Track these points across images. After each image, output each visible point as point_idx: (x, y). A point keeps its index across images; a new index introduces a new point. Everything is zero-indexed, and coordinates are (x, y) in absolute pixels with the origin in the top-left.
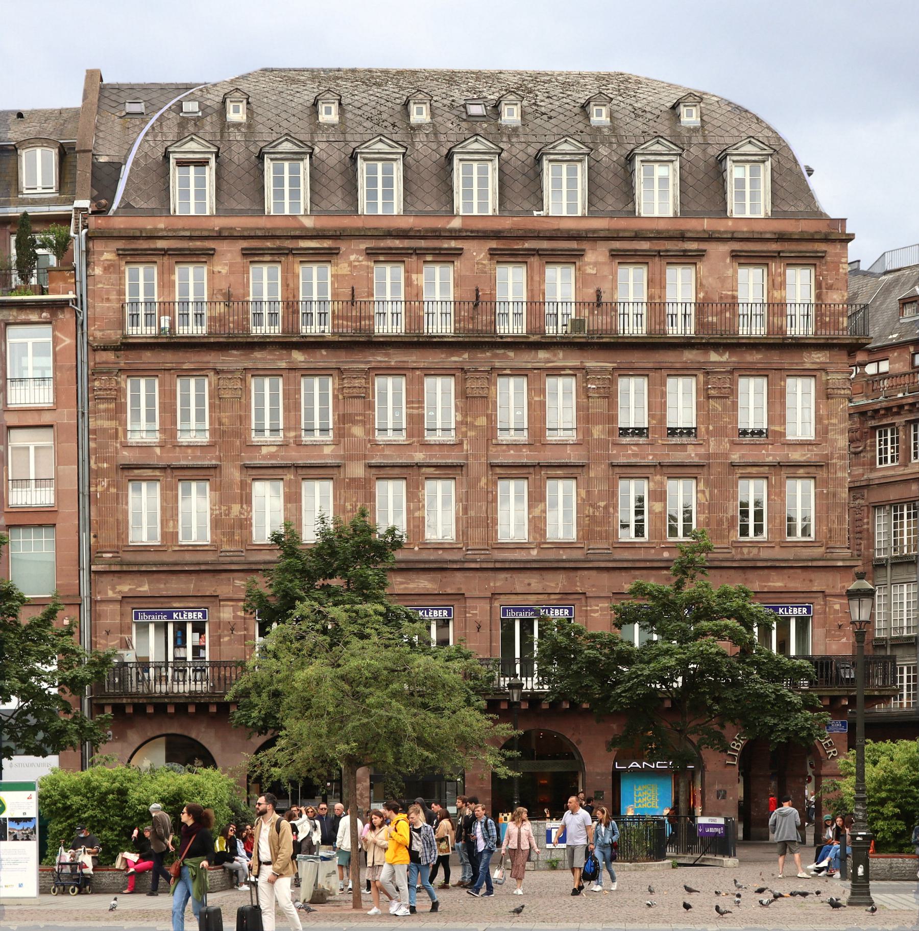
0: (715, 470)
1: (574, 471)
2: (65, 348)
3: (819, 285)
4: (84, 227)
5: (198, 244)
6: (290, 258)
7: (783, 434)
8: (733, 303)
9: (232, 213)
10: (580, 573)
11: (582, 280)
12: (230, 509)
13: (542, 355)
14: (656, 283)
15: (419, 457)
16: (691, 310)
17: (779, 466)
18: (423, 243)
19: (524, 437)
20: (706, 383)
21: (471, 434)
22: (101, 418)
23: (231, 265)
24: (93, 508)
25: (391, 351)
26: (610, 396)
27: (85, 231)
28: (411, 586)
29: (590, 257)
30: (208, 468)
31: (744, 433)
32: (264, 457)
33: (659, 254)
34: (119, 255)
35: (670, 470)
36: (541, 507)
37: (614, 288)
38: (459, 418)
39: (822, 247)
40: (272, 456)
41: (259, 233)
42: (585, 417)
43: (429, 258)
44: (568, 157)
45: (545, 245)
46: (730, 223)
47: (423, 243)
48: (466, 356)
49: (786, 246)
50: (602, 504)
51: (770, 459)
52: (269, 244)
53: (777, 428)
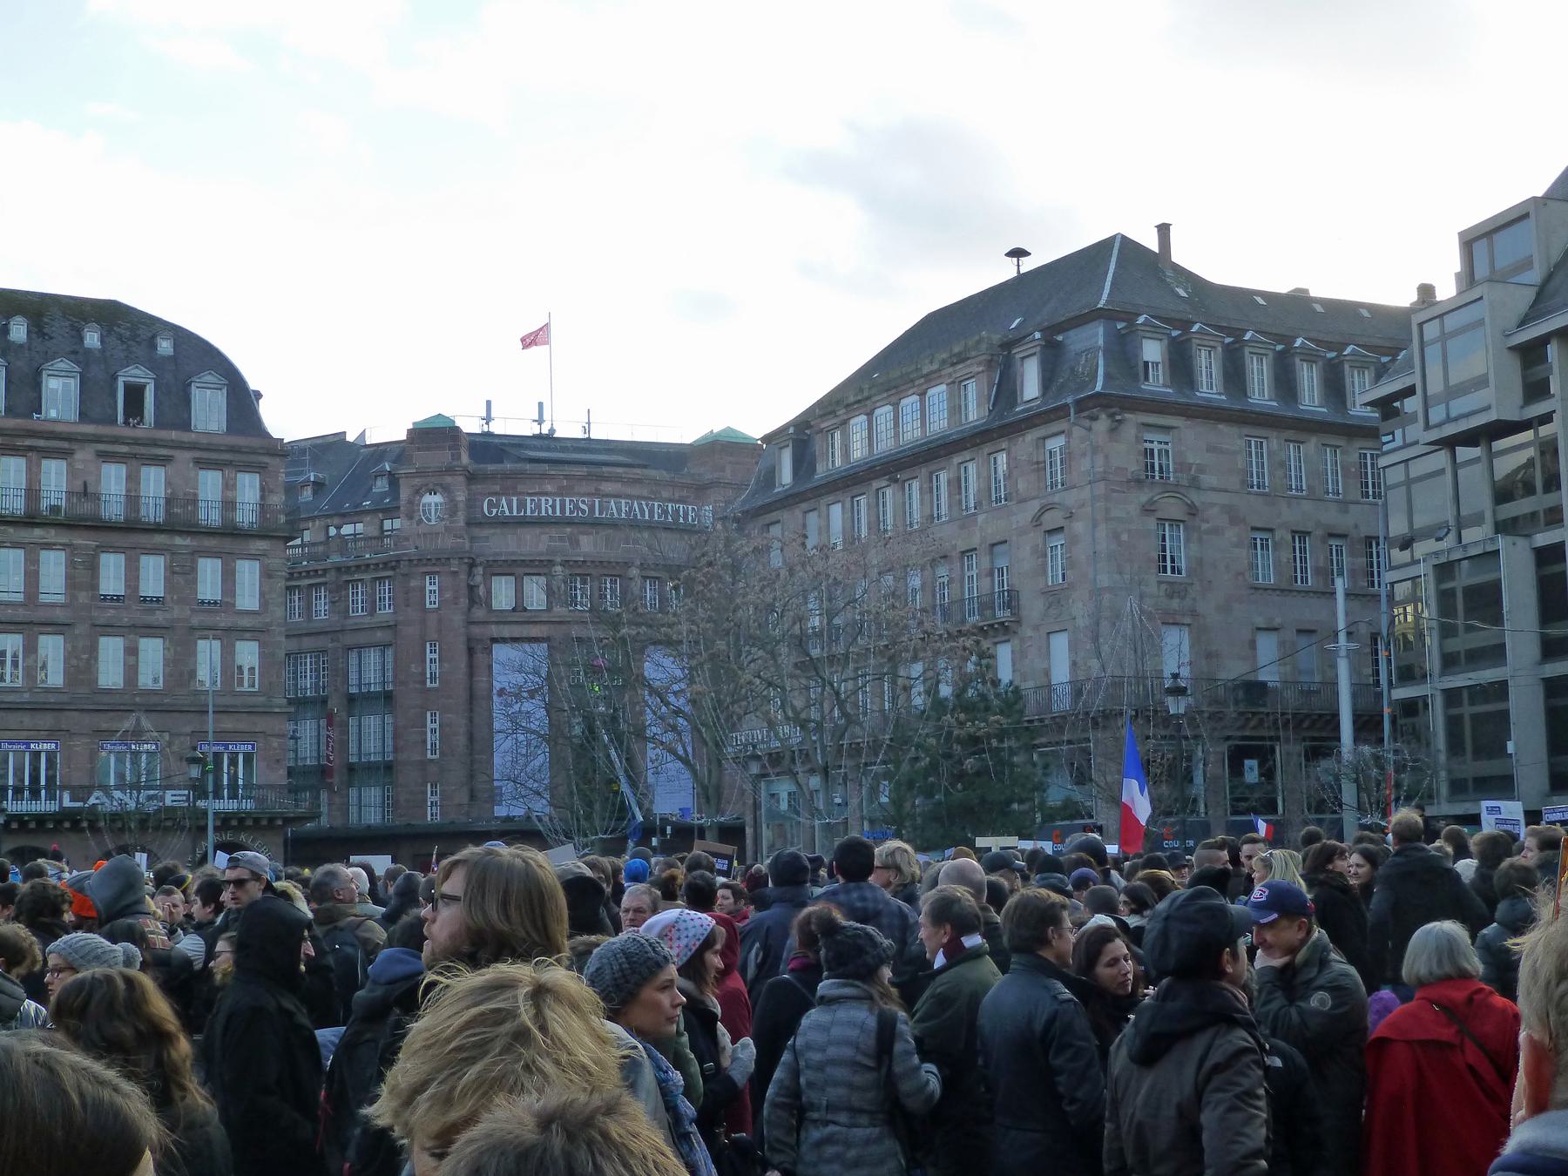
3: (262, 489)
7: (234, 605)
8: (194, 500)
10: (67, 713)
11: (72, 473)
13: (38, 532)
14: (133, 479)
16: (162, 502)
17: (228, 630)
19: (20, 598)
20: (172, 562)
26: (93, 568)
29: (79, 456)
31: (203, 602)
33: (134, 456)
35: (143, 630)
36: (33, 656)
37: (98, 481)
39: (266, 459)
42: (72, 584)
44: (63, 374)
45: (41, 443)
46: (193, 436)
49: (238, 457)
50: (85, 656)
51: (222, 625)
53: (229, 600)
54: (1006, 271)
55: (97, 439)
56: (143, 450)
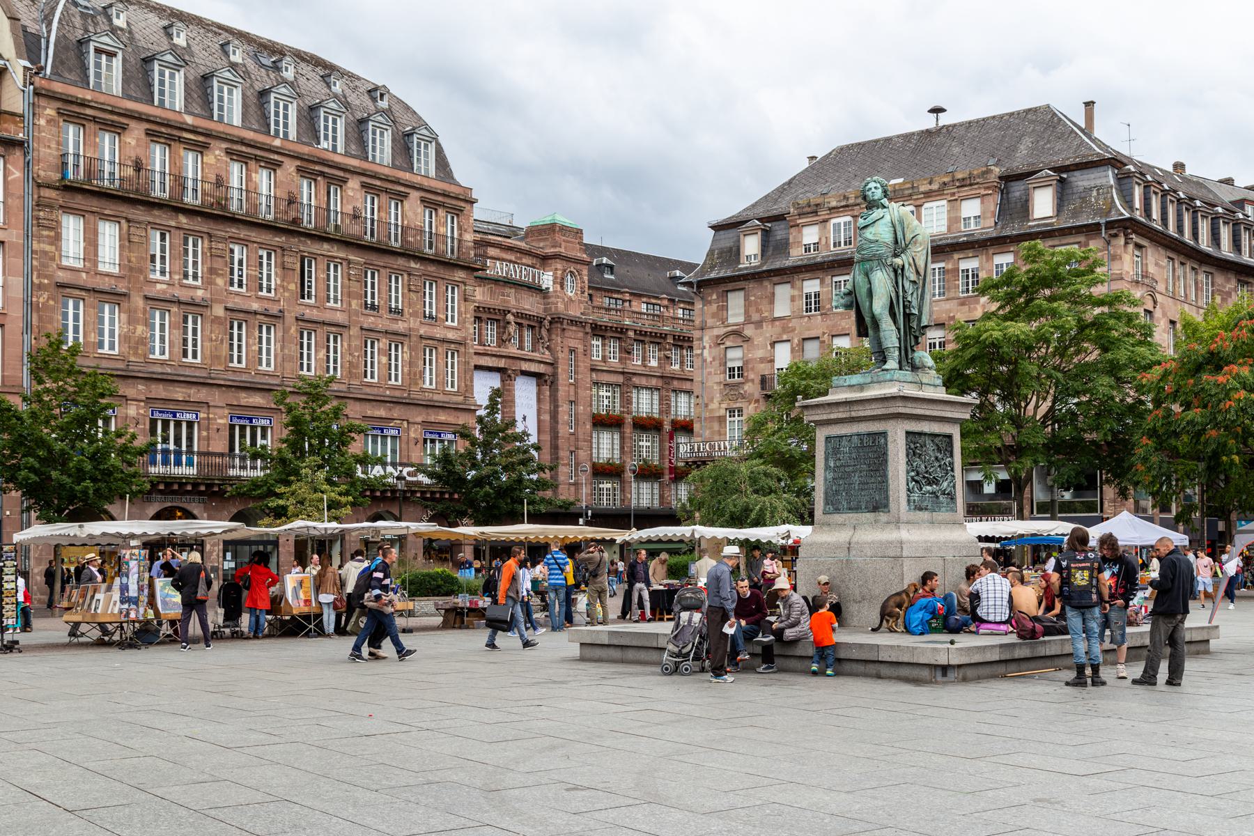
0: (414, 339)
1: (341, 329)
2: (14, 180)
3: (460, 228)
4: (31, 84)
5: (115, 118)
6: (177, 144)
9: (130, 98)
12: (135, 329)
13: (326, 246)
15: (255, 306)
18: (258, 153)
20: (409, 281)
21: (286, 294)
22: (44, 242)
23: (138, 140)
24: (35, 315)
25: (241, 226)
27: (32, 87)
28: (251, 400)
30: (120, 295)
32: (158, 291)
34: (59, 113)
38: (279, 282)
39: (462, 204)
40: (164, 292)
41: (158, 120)
43: (263, 164)
45: (326, 170)
47: (258, 153)
48: (284, 238)
50: (356, 354)
52: (163, 130)
54: (929, 122)
55: (362, 173)
56: (390, 186)
